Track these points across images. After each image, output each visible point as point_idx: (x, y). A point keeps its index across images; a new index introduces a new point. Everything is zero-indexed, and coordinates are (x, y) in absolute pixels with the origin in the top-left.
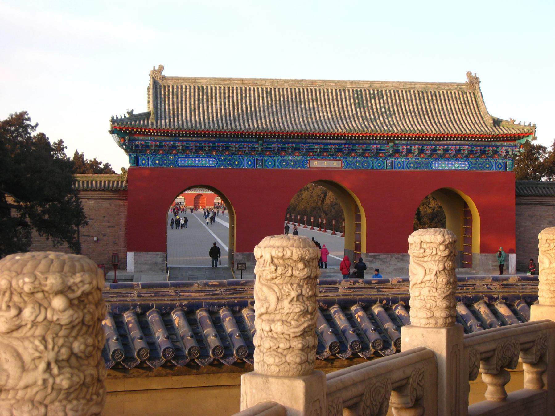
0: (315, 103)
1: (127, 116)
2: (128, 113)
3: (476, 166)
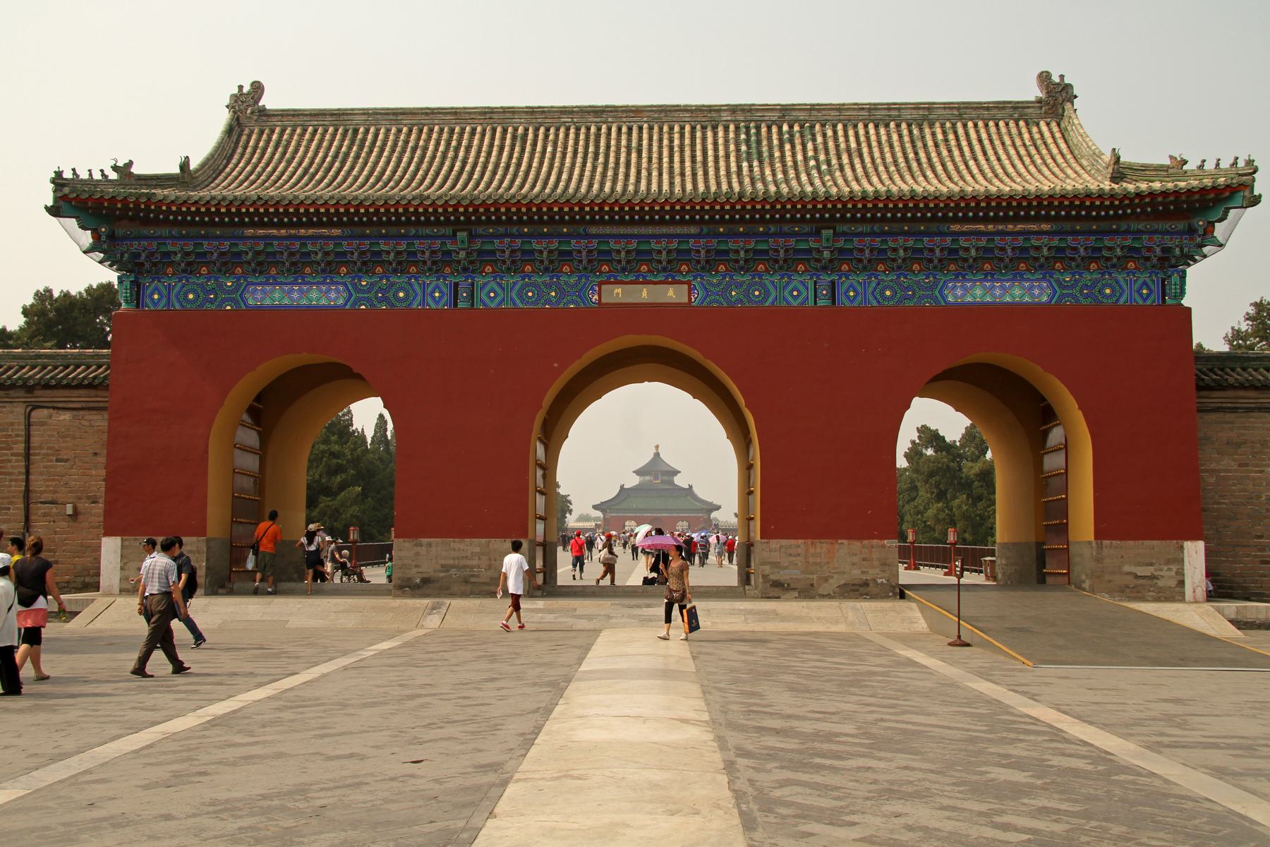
0: (634, 156)
1: (113, 176)
2: (115, 168)
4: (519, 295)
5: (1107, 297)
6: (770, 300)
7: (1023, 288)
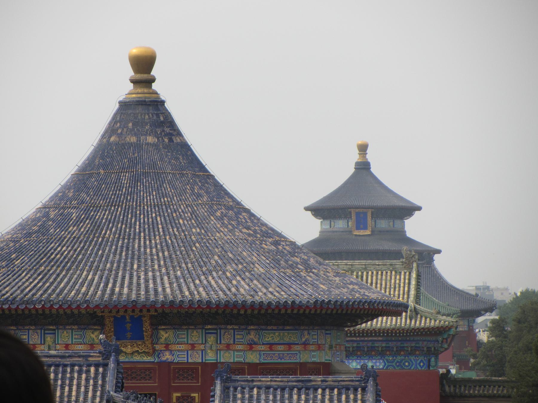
3: (394, 364)
5: (407, 366)
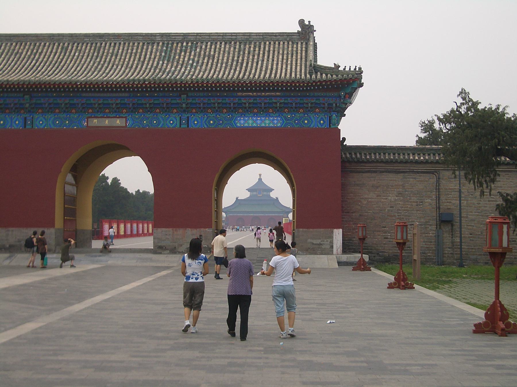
4: (53, 123)
6: (161, 125)
7: (270, 120)
